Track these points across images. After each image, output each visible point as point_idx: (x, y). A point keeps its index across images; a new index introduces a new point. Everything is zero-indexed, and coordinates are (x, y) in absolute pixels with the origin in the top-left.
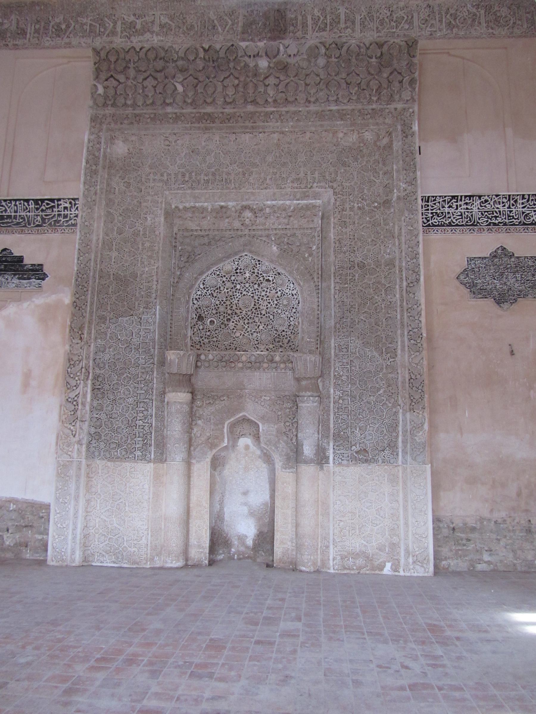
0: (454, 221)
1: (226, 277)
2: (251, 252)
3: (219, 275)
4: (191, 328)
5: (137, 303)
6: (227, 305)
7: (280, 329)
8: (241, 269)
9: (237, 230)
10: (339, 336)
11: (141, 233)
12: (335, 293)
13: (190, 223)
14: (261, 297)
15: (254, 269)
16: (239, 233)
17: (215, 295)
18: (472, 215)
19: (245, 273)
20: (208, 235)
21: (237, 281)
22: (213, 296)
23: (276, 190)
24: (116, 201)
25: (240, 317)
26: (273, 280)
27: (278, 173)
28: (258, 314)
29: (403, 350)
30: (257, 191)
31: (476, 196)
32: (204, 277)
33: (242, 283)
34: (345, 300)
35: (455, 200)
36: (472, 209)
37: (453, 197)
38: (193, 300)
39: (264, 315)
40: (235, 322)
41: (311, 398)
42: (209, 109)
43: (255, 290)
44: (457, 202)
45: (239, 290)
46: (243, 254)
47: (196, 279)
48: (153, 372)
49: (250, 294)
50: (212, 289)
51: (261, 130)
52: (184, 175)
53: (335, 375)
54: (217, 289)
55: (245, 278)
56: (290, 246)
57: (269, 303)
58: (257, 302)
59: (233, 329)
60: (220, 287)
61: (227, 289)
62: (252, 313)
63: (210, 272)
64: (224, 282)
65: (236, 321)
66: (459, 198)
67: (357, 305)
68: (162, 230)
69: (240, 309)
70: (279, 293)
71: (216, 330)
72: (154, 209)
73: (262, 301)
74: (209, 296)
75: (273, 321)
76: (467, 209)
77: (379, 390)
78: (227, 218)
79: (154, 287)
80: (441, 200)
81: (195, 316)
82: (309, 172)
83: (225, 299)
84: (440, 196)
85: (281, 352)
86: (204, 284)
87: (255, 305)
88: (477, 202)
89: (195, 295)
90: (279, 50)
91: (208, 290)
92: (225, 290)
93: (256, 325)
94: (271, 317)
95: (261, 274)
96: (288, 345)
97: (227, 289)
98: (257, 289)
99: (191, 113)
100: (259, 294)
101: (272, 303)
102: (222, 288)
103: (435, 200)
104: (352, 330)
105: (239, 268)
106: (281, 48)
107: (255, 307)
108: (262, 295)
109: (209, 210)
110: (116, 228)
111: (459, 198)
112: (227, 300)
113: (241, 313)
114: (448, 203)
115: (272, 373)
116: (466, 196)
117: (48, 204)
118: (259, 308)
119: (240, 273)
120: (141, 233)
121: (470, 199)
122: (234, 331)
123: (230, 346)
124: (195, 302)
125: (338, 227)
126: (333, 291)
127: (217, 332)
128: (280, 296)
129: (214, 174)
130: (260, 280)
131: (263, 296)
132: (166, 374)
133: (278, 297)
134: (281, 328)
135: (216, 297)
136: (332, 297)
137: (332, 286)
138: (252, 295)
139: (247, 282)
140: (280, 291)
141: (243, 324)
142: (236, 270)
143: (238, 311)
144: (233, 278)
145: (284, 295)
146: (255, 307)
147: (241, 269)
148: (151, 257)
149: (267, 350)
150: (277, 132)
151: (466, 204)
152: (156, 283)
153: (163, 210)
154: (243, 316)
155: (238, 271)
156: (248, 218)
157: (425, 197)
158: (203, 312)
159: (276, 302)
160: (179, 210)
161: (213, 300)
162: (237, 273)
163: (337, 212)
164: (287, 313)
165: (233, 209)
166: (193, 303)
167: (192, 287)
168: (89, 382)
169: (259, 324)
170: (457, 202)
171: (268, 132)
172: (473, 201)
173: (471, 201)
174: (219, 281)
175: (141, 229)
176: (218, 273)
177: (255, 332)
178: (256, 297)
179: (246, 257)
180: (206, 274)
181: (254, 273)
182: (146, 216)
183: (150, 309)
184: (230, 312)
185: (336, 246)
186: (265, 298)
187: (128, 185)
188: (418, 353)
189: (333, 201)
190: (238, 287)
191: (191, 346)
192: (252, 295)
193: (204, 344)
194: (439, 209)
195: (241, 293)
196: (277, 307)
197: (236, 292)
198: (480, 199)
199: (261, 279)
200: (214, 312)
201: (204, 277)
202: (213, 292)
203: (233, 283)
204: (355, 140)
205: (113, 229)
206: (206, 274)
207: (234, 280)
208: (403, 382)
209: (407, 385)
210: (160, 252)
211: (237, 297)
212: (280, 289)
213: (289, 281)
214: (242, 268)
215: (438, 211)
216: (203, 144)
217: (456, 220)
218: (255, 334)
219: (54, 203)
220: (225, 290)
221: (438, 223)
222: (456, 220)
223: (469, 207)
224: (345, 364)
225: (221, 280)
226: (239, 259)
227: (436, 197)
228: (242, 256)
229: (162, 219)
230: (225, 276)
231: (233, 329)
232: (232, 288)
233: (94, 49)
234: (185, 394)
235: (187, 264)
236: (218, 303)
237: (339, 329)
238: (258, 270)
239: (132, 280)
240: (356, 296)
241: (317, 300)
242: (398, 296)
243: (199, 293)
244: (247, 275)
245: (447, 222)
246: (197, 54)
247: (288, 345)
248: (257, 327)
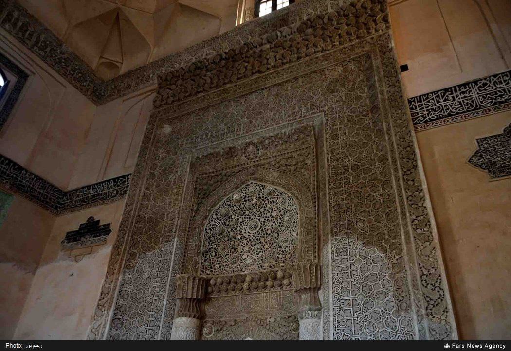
0: (454, 111)
1: (237, 205)
2: (255, 179)
3: (230, 205)
4: (203, 254)
5: (161, 238)
6: (237, 231)
7: (284, 245)
8: (249, 197)
9: (244, 164)
10: (336, 239)
11: (172, 183)
12: (330, 198)
13: (208, 167)
14: (267, 219)
15: (259, 195)
16: (246, 166)
17: (227, 223)
18: (472, 101)
19: (252, 200)
20: (221, 174)
21: (246, 208)
22: (226, 225)
23: (275, 126)
24: (159, 164)
25: (248, 239)
26: (276, 201)
27: (278, 113)
28: (264, 235)
29: (408, 242)
30: (260, 131)
31: (471, 83)
32: (216, 208)
33: (250, 209)
34: (341, 203)
35: (450, 93)
36: (470, 96)
37: (446, 90)
38: (206, 230)
39: (269, 234)
40: (244, 245)
41: (310, 312)
43: (261, 213)
44: (452, 94)
45: (248, 215)
46: (249, 183)
47: (210, 211)
48: (164, 298)
49: (257, 217)
50: (224, 218)
51: (263, 87)
52: (207, 135)
53: (333, 283)
54: (229, 218)
55: (253, 204)
56: (288, 167)
57: (274, 222)
58: (263, 223)
59: (242, 252)
60: (231, 216)
61: (238, 217)
62: (259, 235)
63: (220, 203)
64: (234, 211)
65: (244, 244)
66: (453, 89)
67: (353, 205)
68: (187, 178)
69: (248, 232)
70: (282, 211)
71: (227, 255)
72: (184, 164)
73: (268, 222)
74: (222, 225)
75: (277, 239)
76: (465, 97)
77: (386, 294)
78: (236, 156)
79: (175, 223)
80: (434, 96)
81: (208, 244)
82: (303, 106)
83: (235, 226)
84: (432, 93)
85: (283, 266)
86: (216, 215)
87: (261, 227)
88: (475, 88)
89: (209, 225)
90: (277, 35)
91: (221, 220)
92: (236, 217)
93: (262, 245)
94: (276, 235)
95: (266, 198)
96: (290, 259)
97: (238, 217)
98: (264, 212)
99: (215, 92)
100: (265, 216)
101: (276, 222)
102: (233, 217)
103: (426, 99)
104: (349, 231)
105: (247, 196)
106: (279, 34)
107: (262, 228)
108: (267, 216)
109: (221, 153)
110: (155, 184)
111: (453, 89)
112: (237, 227)
113: (249, 236)
114: (443, 97)
115: (278, 293)
116: (460, 86)
117: (121, 180)
118: (265, 229)
119: (248, 200)
120: (172, 183)
121: (465, 88)
122: (242, 253)
123: (237, 268)
124: (209, 231)
125: (330, 141)
126: (328, 196)
127: (227, 256)
128: (283, 214)
130: (266, 204)
131: (268, 217)
132: (178, 300)
133: (281, 215)
134: (285, 245)
135: (228, 225)
136: (328, 202)
137: (327, 192)
138: (259, 218)
139: (255, 207)
140: (283, 209)
141: (250, 246)
142: (244, 199)
143: (246, 235)
144: (242, 206)
145: (287, 212)
146: (262, 228)
147: (249, 197)
148: (176, 200)
149: (270, 267)
150: (276, 85)
151: (463, 93)
152: (177, 219)
153: (189, 163)
154: (250, 238)
155: (246, 199)
156: (251, 152)
157: (416, 97)
158: (216, 240)
159: (280, 221)
160: (200, 159)
161: (225, 229)
162: (246, 201)
163: (329, 129)
164: (289, 229)
165: (239, 148)
166: (207, 232)
167: (206, 217)
168: (111, 313)
169: (264, 243)
170: (452, 94)
171: (268, 87)
172: (470, 88)
173: (468, 89)
174: (230, 210)
175: (172, 180)
176: (229, 203)
177: (260, 252)
178: (262, 220)
179: (251, 185)
180: (218, 205)
181: (260, 198)
182: (177, 170)
183: (170, 241)
185: (330, 156)
186: (270, 219)
187: (168, 152)
188: (428, 243)
189: (325, 121)
190: (247, 213)
191: (201, 271)
192: (259, 218)
193: (215, 269)
194: (435, 105)
195: (250, 218)
196: (281, 224)
197: (245, 218)
198: (477, 85)
199: (266, 202)
200: (226, 239)
201: (216, 208)
202: (226, 221)
203: (242, 210)
204: (340, 72)
205: (153, 184)
206: (218, 205)
207: (243, 208)
208: (414, 280)
209: (419, 283)
210: (184, 195)
211: (246, 222)
212: (283, 207)
213: (289, 197)
214: (250, 196)
215: (434, 107)
217: (456, 110)
218: (261, 254)
219: (125, 178)
220: (236, 217)
221: (436, 117)
222: (456, 110)
223: (467, 95)
224: (345, 269)
225: (232, 210)
226: (246, 188)
227: (428, 94)
228: (248, 185)
229: (188, 170)
230: (235, 205)
231: (242, 252)
232: (242, 215)
234: (190, 319)
235: (203, 201)
236: (230, 230)
237: (336, 232)
238: (263, 194)
239: (160, 220)
240: (352, 197)
241: (313, 209)
242: (395, 187)
243: (212, 223)
244: (255, 201)
245: (446, 114)
247: (290, 259)
248: (262, 247)
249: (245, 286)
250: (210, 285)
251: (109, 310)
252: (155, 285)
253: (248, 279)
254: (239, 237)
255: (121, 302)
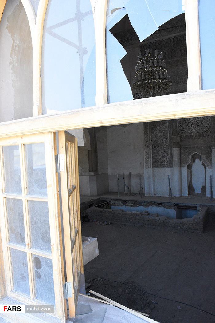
42: (177, 58)
99: (171, 61)
129: (180, 80)
168: (151, 147)
184: (189, 122)
200: (185, 122)
216: (176, 70)
233: (140, 46)
246: (171, 40)
249: (193, 138)
250: (181, 137)
251: (150, 146)
252: (164, 138)
253: (195, 136)
254: (189, 122)
255: (153, 143)
